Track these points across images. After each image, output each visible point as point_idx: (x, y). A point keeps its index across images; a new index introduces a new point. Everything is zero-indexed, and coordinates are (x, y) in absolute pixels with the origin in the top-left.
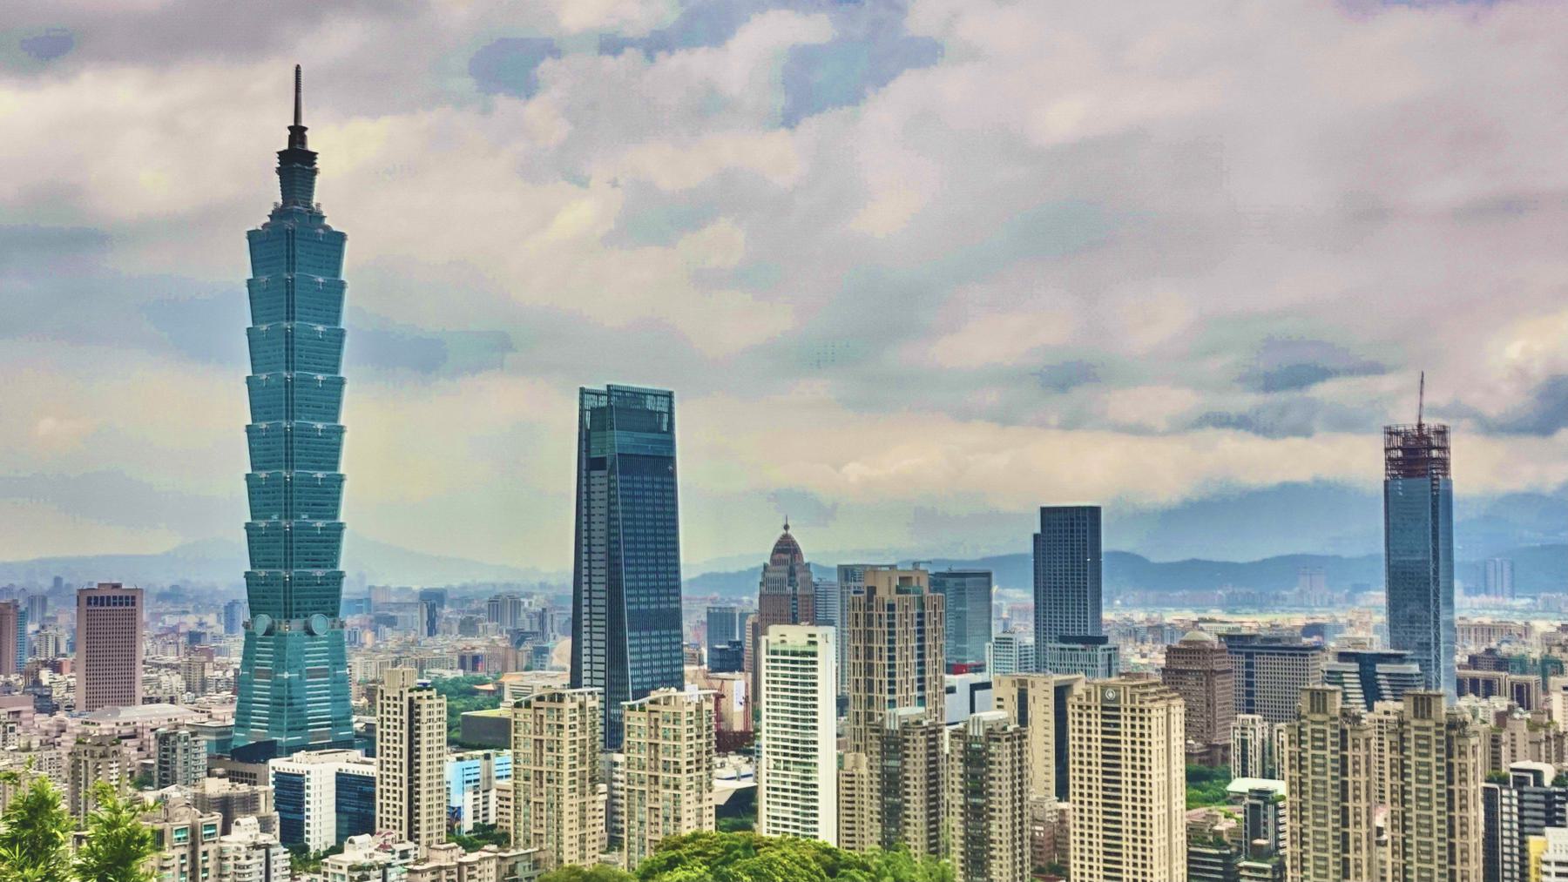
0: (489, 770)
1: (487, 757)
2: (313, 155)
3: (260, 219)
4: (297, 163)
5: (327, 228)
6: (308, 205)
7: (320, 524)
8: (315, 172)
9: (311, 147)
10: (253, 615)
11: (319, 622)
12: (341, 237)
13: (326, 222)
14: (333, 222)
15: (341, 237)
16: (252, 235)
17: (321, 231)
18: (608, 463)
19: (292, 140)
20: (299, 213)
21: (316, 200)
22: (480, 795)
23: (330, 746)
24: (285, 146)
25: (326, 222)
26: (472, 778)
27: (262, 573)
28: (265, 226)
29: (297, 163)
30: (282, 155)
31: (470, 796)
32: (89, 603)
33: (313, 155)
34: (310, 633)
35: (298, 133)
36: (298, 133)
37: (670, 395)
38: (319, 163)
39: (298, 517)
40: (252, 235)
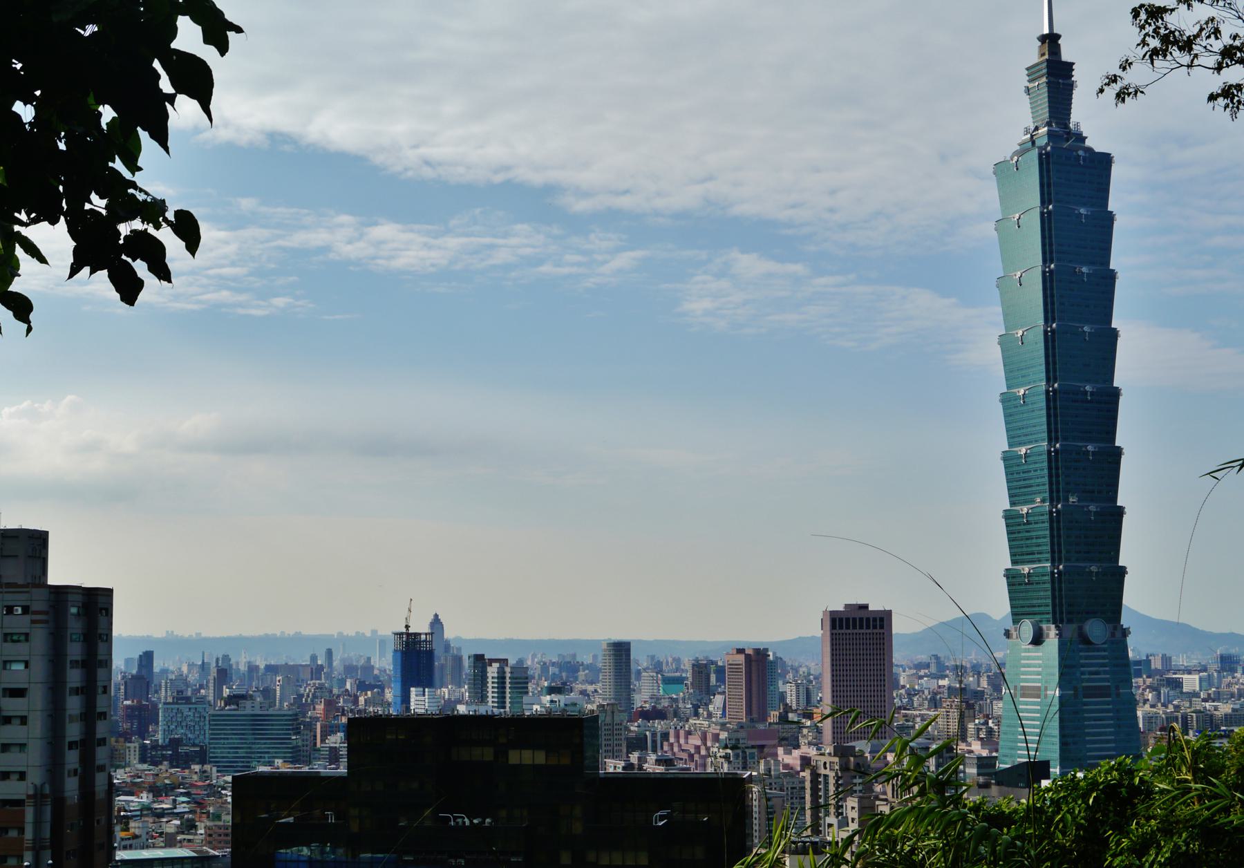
2: (1070, 66)
5: (1090, 150)
6: (1066, 126)
9: (1065, 57)
10: (1015, 622)
11: (1095, 629)
12: (1105, 161)
13: (1088, 143)
14: (1096, 142)
15: (1105, 161)
17: (1081, 153)
25: (1088, 143)
27: (1026, 569)
32: (833, 626)
33: (1070, 66)
34: (1085, 640)
35: (1051, 41)
36: (1051, 41)
38: (1077, 75)
39: (1067, 500)
40: (1000, 169)
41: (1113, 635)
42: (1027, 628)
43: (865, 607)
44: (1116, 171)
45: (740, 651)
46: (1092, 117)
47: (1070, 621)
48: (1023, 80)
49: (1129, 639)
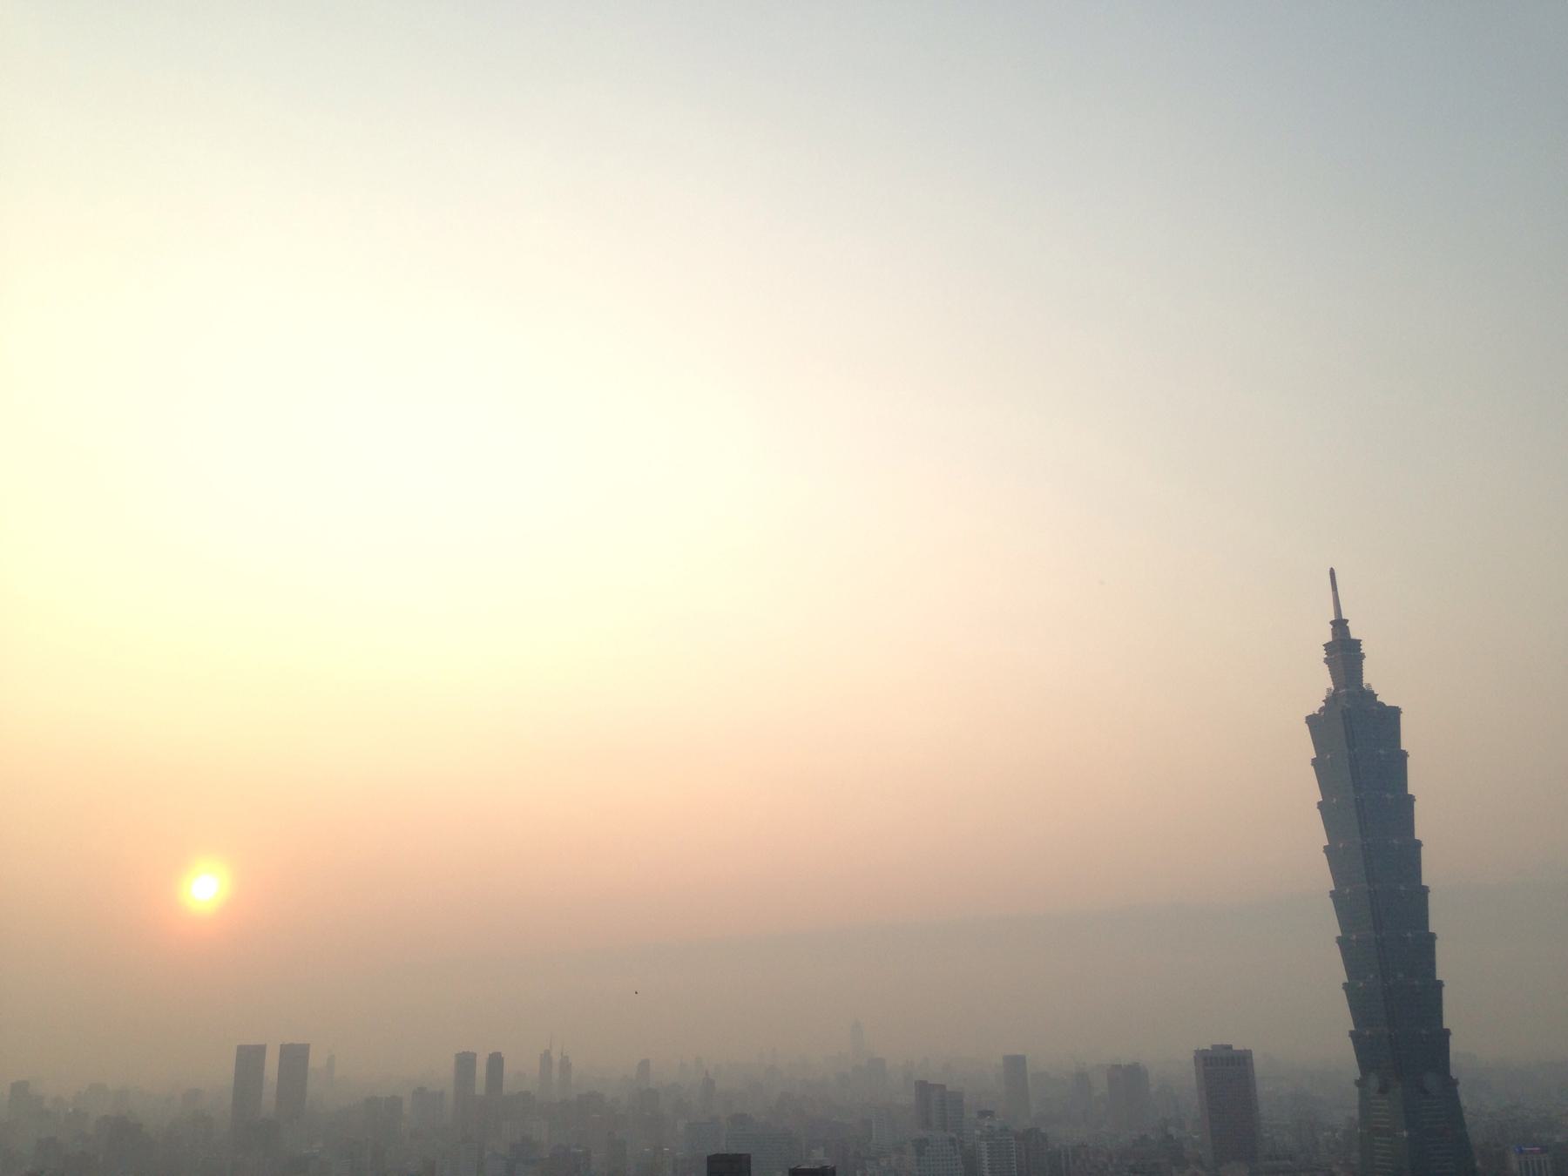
2: (1357, 643)
3: (1315, 704)
4: (1344, 652)
8: (1362, 656)
9: (1354, 635)
12: (1396, 712)
14: (1386, 698)
15: (1396, 712)
16: (1311, 720)
21: (1367, 679)
24: (1329, 638)
28: (1321, 710)
29: (1344, 652)
30: (1327, 646)
33: (1357, 643)
35: (1340, 625)
36: (1340, 625)
38: (1364, 649)
40: (1311, 720)
42: (1374, 1082)
43: (1230, 1047)
44: (1403, 718)
45: (1118, 1067)
46: (1382, 677)
48: (1323, 654)
49: (1460, 1088)
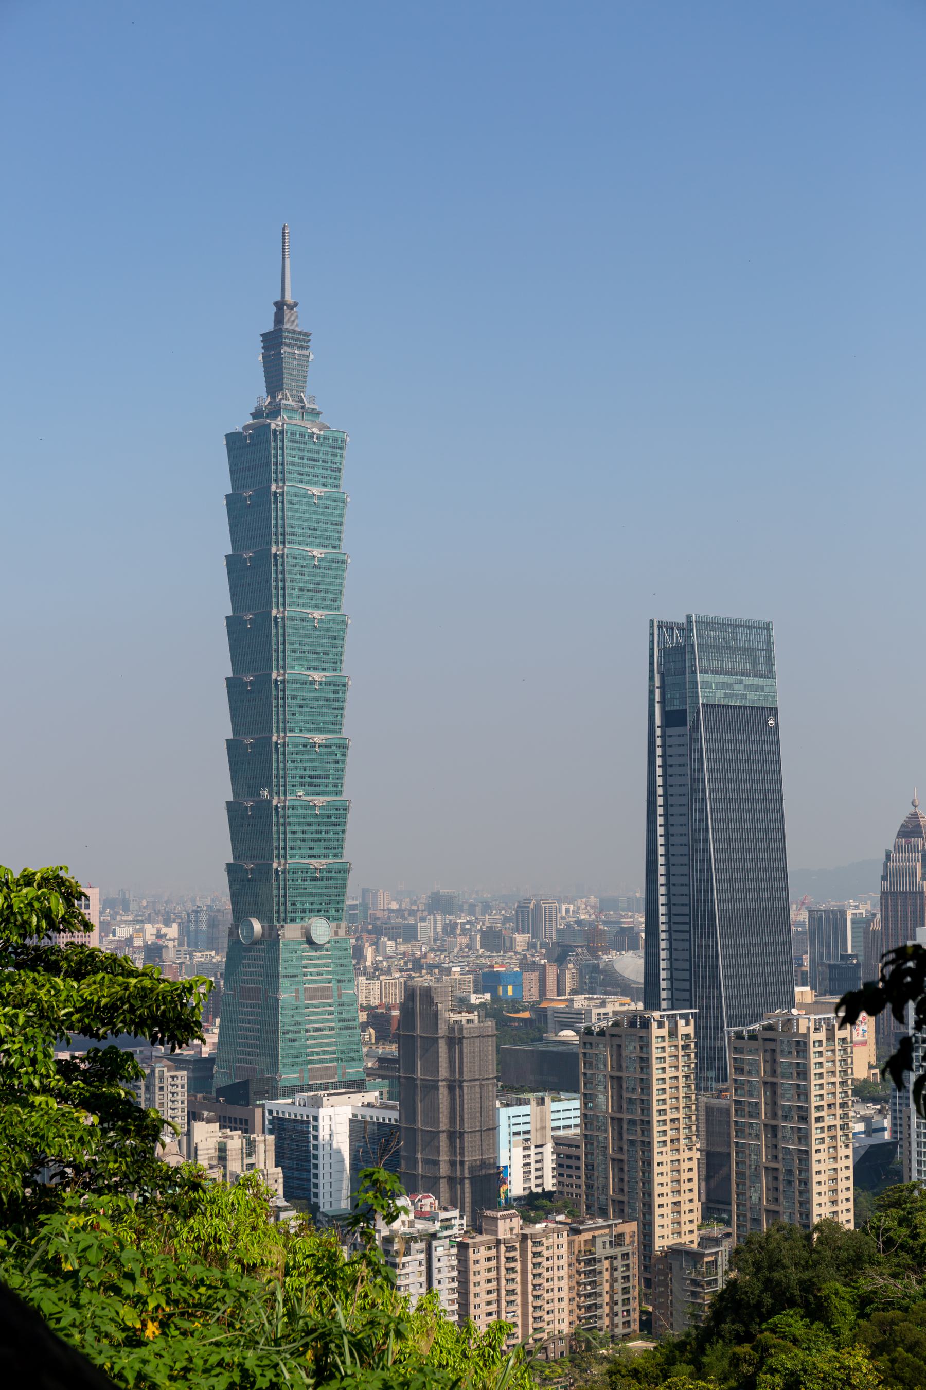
0: (543, 1119)
1: (541, 1102)
3: (240, 420)
7: (319, 800)
16: (233, 440)
18: (690, 718)
19: (279, 319)
20: (290, 409)
22: (533, 1151)
23: (335, 1086)
24: (270, 327)
26: (521, 1128)
30: (266, 337)
31: (518, 1152)
37: (767, 628)
40: (233, 440)
41: (336, 933)
47: (293, 920)
